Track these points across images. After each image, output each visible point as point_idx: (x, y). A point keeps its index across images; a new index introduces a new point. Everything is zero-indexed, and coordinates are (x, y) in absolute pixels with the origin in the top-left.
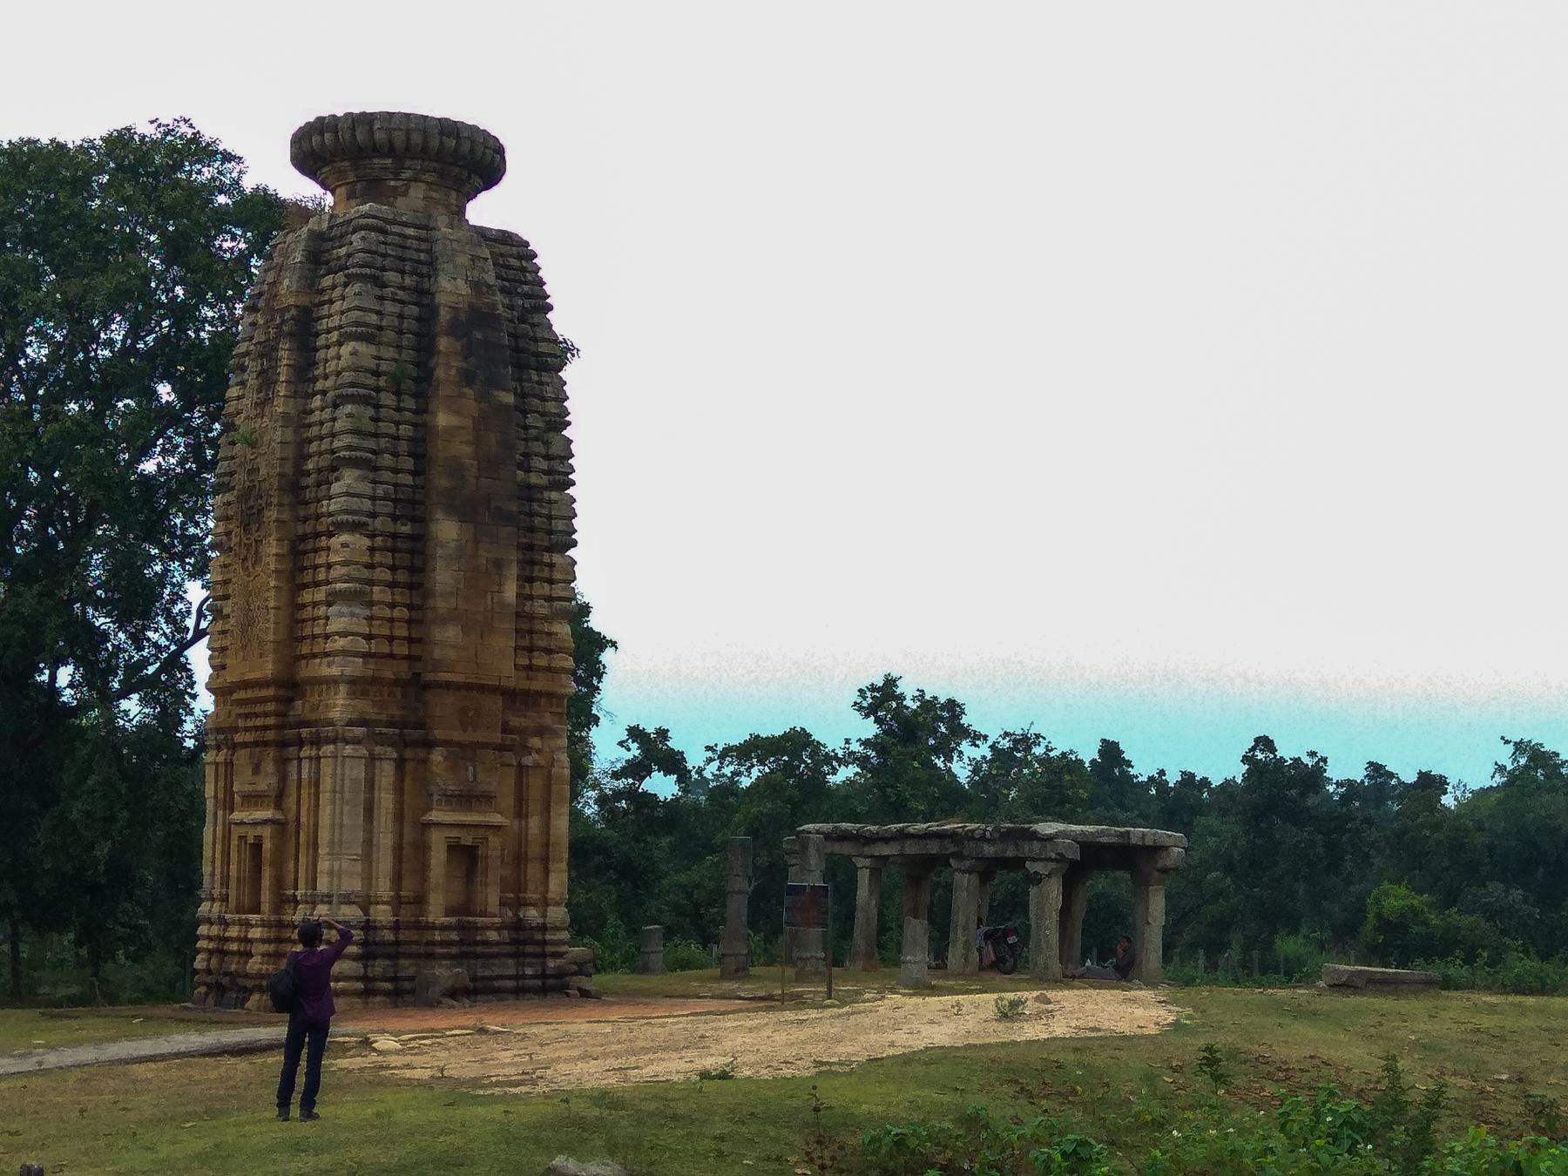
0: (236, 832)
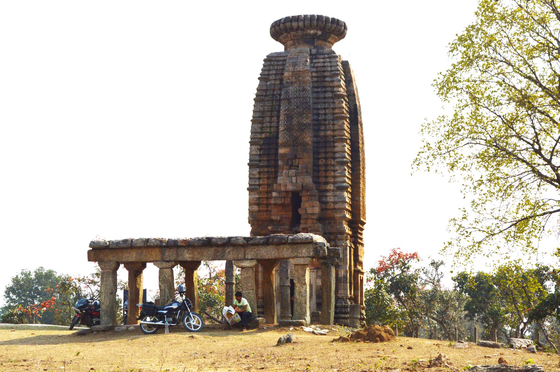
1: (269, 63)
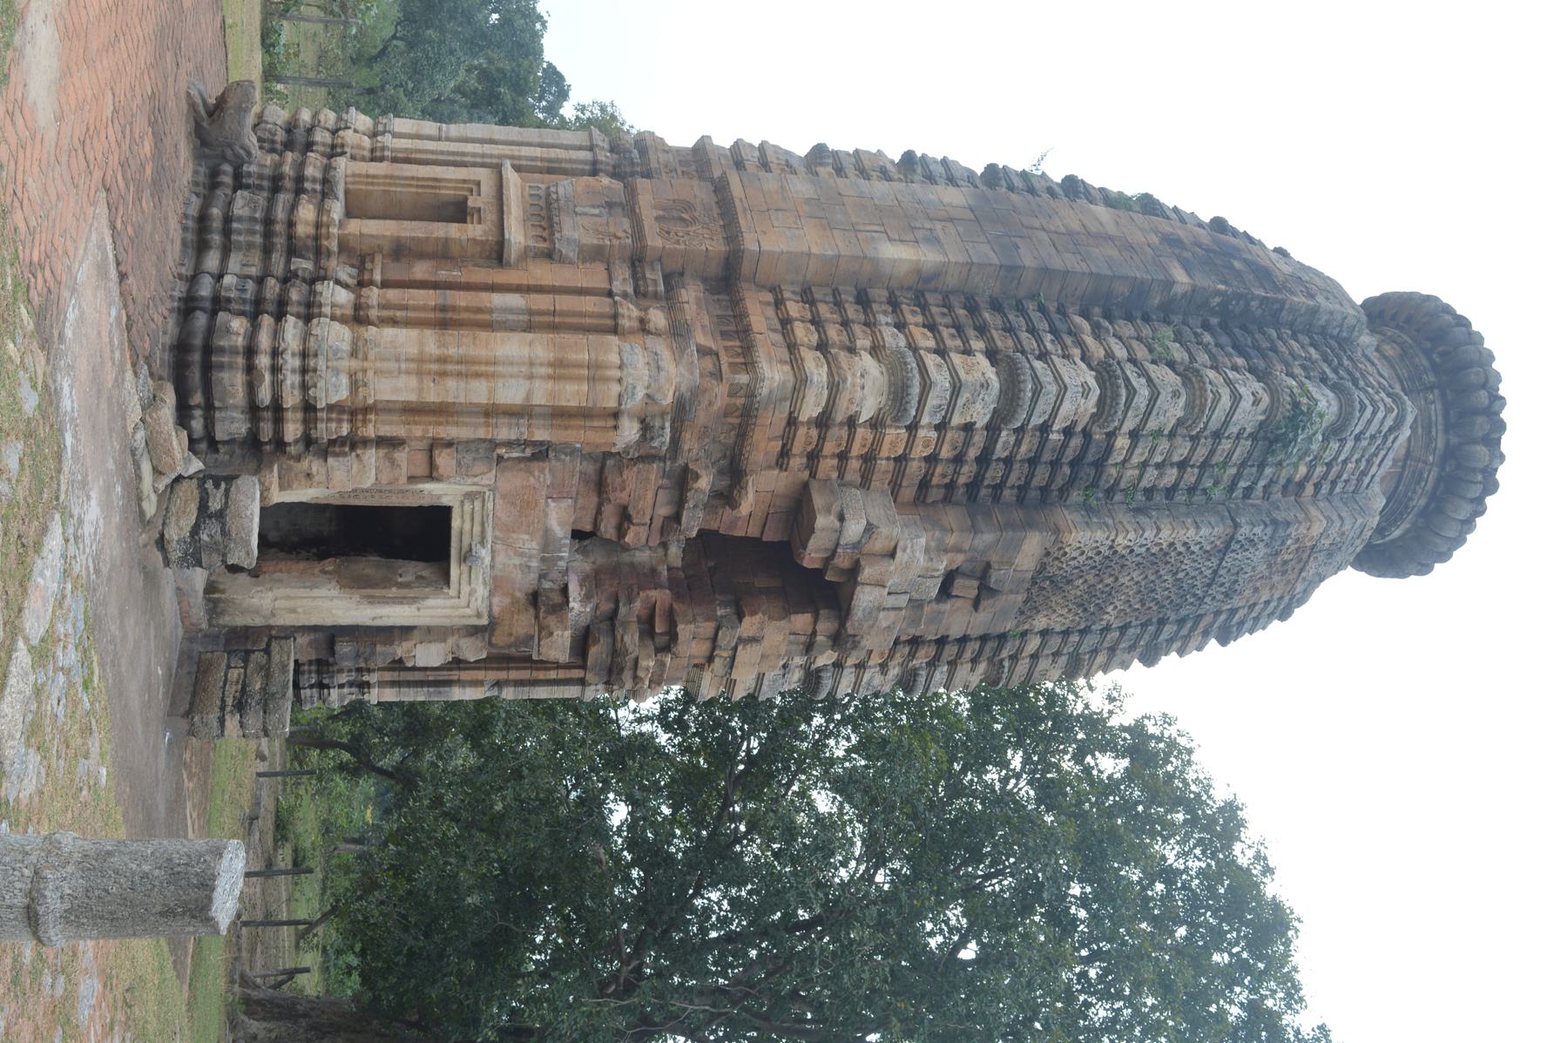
0: (483, 175)
1: (1385, 429)
